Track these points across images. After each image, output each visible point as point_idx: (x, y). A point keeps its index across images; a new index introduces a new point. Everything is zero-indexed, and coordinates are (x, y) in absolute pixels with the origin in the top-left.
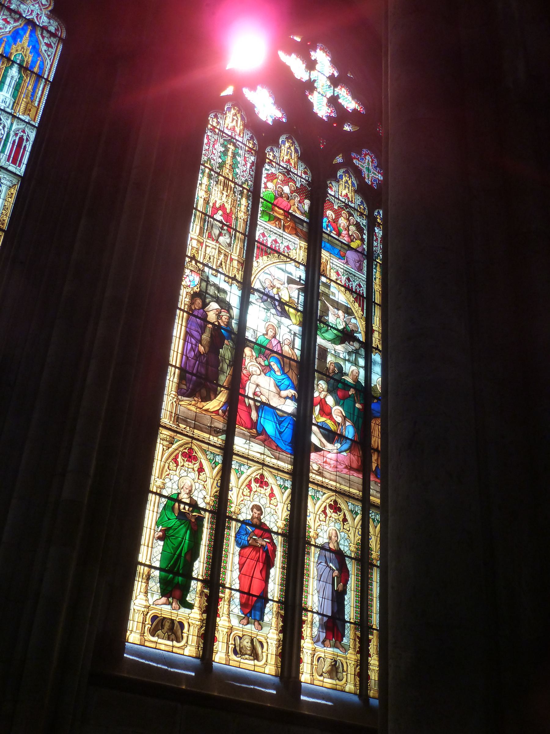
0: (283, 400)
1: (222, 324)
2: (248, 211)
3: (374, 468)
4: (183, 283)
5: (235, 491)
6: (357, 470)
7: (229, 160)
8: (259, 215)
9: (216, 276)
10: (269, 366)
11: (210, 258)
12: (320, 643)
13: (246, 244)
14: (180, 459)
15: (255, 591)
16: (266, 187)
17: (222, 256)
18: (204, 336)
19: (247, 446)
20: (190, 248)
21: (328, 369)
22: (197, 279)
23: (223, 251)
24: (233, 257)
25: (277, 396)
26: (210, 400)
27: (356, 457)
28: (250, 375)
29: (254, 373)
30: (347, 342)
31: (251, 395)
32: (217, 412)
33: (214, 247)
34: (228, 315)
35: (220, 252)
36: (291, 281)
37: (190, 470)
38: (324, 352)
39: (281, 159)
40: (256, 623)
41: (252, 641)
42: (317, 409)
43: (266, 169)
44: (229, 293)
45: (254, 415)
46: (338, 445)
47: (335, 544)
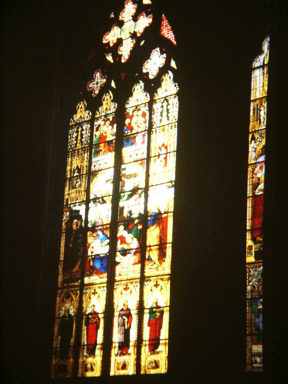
0: (103, 247)
1: (78, 228)
2: (87, 158)
3: (147, 257)
4: (63, 220)
5: (85, 302)
6: (138, 263)
7: (79, 138)
8: (93, 156)
9: (75, 206)
10: (98, 235)
11: (73, 199)
12: (118, 356)
13: (87, 179)
14: (65, 300)
15: (93, 343)
16: (96, 136)
17: (78, 193)
18: (72, 239)
19: (89, 280)
20: (65, 200)
21: (124, 217)
22: (68, 213)
23: (78, 191)
24: (82, 190)
25: (101, 247)
26: (75, 267)
27: (138, 256)
28: (90, 244)
29: (92, 242)
30: (135, 195)
31: (90, 255)
32: (77, 271)
33: (74, 191)
34: (80, 221)
35: (77, 192)
36: (107, 181)
37: (68, 302)
38: (122, 209)
39: (103, 112)
40: (93, 356)
41: (91, 364)
42: (119, 242)
43: (96, 125)
44: (80, 210)
45: (91, 264)
46: (128, 255)
47: (127, 307)
